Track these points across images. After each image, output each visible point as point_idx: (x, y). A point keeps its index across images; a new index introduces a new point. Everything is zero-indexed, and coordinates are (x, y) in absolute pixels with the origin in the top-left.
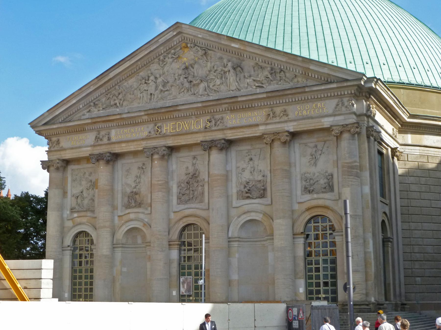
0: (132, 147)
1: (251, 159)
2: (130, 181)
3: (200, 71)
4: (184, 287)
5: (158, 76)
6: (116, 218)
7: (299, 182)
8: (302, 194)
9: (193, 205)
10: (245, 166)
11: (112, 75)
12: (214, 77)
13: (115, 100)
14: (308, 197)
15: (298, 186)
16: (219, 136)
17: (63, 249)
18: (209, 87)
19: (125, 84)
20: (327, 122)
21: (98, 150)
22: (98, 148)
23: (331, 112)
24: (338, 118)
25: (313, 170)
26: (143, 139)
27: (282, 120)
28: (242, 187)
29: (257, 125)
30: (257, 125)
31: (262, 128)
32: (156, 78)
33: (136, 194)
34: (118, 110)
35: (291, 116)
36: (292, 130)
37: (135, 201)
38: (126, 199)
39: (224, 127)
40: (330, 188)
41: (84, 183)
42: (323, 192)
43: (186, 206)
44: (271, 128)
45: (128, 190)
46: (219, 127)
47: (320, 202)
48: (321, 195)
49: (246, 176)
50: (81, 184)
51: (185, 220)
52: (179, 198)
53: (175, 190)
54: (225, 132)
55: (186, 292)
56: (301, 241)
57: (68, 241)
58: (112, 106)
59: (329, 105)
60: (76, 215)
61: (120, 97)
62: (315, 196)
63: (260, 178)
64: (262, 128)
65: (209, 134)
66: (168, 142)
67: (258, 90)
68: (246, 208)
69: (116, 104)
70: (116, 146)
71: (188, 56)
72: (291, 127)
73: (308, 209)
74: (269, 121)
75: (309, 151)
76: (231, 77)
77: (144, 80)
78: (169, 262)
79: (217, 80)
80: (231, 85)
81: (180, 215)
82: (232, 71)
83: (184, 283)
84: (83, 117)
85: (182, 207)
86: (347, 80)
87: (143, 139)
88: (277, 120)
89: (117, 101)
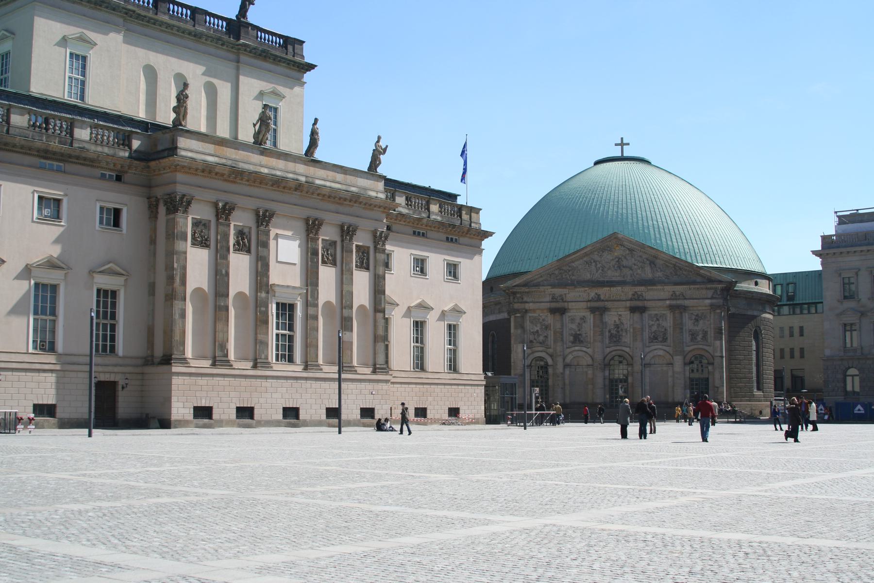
1: (658, 320)
2: (574, 326)
15: (687, 338)
21: (554, 305)
23: (710, 296)
31: (668, 302)
33: (580, 335)
38: (572, 338)
40: (705, 337)
41: (539, 325)
44: (674, 302)
49: (654, 328)
59: (710, 293)
75: (694, 317)
76: (648, 269)
80: (648, 274)
81: (611, 349)
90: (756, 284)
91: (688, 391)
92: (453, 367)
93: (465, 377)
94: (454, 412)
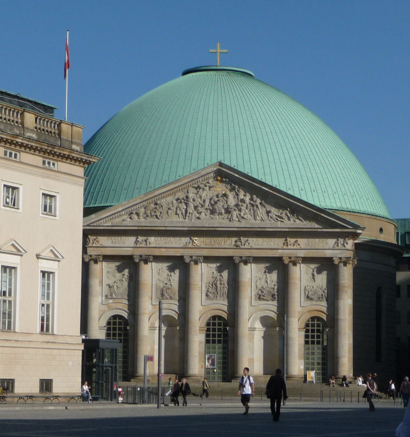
0: (172, 253)
3: (232, 201)
4: (209, 362)
5: (196, 199)
6: (150, 306)
7: (303, 292)
8: (305, 301)
9: (220, 302)
10: (261, 276)
11: (157, 193)
12: (244, 208)
13: (155, 212)
14: (309, 303)
16: (246, 253)
17: (101, 328)
18: (240, 215)
19: (164, 200)
20: (328, 254)
22: (139, 249)
23: (331, 247)
24: (336, 251)
25: (313, 284)
26: (181, 248)
27: (295, 247)
28: (260, 293)
29: (278, 249)
30: (278, 249)
32: (194, 200)
34: (158, 221)
35: (303, 246)
36: (303, 256)
37: (169, 295)
39: (249, 247)
42: (320, 301)
43: (213, 302)
45: (162, 285)
46: (246, 247)
47: (318, 308)
48: (319, 303)
49: (263, 283)
50: (115, 276)
51: (212, 312)
52: (207, 295)
53: (204, 290)
54: (252, 250)
55: (210, 365)
56: (303, 333)
57: (104, 322)
58: (152, 216)
59: (331, 242)
60: (111, 301)
61: (161, 210)
62: (314, 303)
63: (273, 286)
64: (280, 251)
65: (238, 250)
66: (203, 252)
67: (279, 224)
68: (262, 307)
69: (156, 216)
70: (156, 249)
71: (221, 188)
72: (302, 254)
73: (309, 311)
74: (285, 247)
77: (183, 201)
78: (200, 343)
79: (247, 211)
82: (259, 206)
83: (209, 359)
84: (124, 223)
85: (210, 302)
86: (348, 228)
87: (181, 248)
88: (292, 247)
89: (158, 214)
90: (381, 230)
91: (302, 361)
92: (45, 328)
93: (60, 340)
94: (46, 385)
